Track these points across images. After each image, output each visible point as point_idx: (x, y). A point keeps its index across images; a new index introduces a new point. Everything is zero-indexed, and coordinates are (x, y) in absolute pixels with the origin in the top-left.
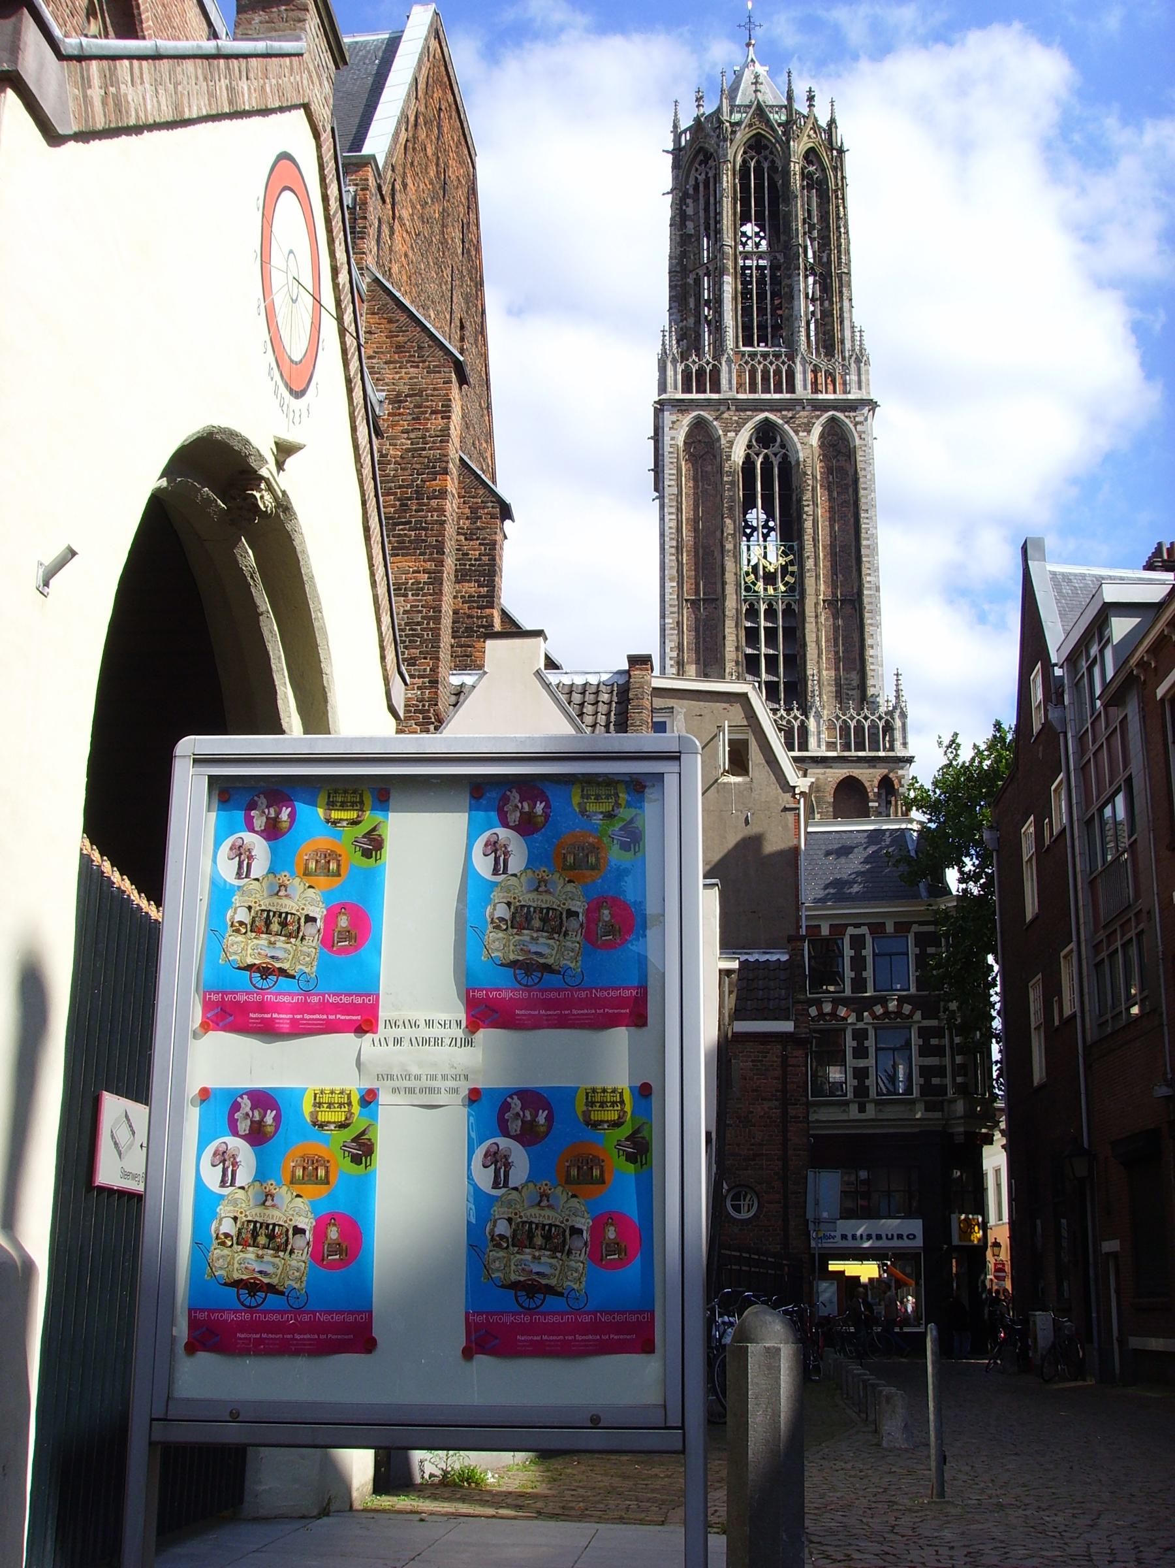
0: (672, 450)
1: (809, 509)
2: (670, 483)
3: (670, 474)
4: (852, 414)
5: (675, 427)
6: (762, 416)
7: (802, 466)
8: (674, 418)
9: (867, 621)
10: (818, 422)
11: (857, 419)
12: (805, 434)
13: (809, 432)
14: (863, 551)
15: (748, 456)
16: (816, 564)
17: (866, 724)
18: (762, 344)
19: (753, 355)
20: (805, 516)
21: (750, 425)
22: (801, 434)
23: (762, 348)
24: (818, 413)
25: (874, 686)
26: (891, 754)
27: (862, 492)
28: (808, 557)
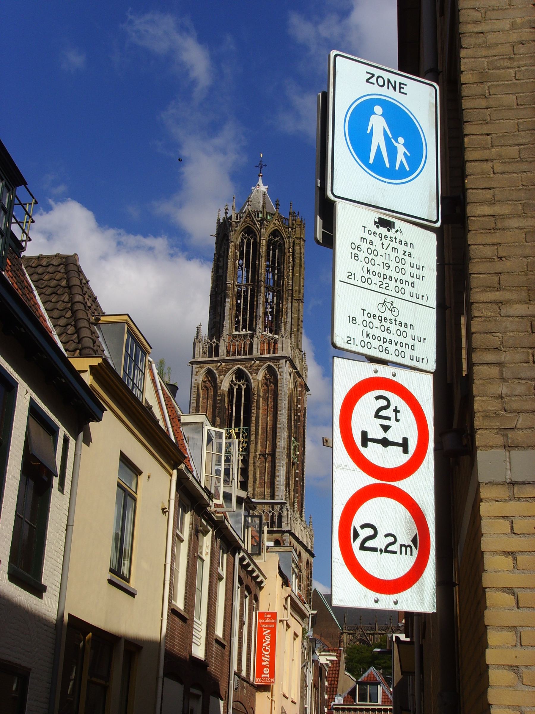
0: (195, 386)
1: (254, 411)
2: (193, 402)
3: (194, 397)
4: (277, 364)
5: (197, 374)
6: (237, 367)
7: (253, 390)
8: (197, 370)
9: (277, 464)
10: (261, 368)
11: (280, 366)
12: (255, 374)
13: (257, 373)
14: (278, 430)
15: (231, 386)
16: (256, 438)
17: (270, 515)
18: (244, 330)
19: (235, 336)
20: (252, 415)
21: (231, 371)
22: (253, 375)
23: (243, 332)
24: (262, 364)
25: (278, 495)
26: (280, 529)
27: (279, 401)
28: (252, 434)
